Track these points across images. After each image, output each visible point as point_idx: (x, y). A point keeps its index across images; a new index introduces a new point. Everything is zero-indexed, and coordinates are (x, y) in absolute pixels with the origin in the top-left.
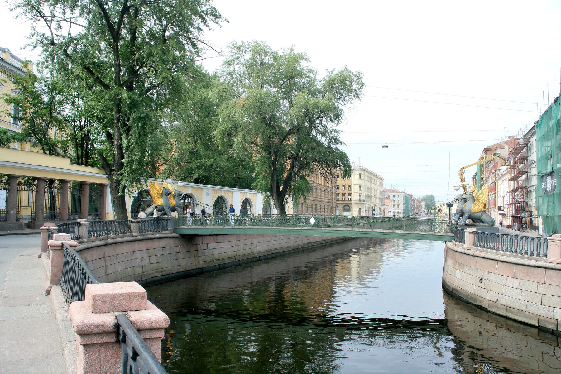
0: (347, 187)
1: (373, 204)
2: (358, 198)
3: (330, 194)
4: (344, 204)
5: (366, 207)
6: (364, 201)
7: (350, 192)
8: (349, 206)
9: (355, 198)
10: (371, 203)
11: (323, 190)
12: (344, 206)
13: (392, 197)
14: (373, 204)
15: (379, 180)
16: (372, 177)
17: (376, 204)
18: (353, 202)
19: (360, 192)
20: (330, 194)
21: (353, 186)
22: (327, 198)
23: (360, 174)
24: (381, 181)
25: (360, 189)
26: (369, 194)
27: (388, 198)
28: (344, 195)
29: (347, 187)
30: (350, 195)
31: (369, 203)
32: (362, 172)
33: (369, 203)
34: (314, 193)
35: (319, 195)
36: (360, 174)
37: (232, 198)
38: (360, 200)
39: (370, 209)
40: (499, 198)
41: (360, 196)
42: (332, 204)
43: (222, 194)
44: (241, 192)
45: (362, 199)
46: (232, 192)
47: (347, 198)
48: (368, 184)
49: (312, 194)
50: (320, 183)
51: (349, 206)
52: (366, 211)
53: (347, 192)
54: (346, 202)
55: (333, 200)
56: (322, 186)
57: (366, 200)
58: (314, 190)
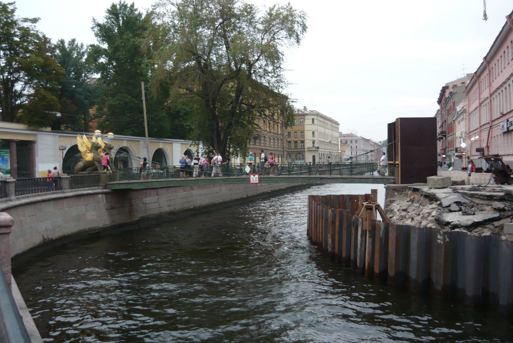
0: (299, 134)
1: (328, 151)
2: (311, 145)
3: (280, 142)
4: (297, 152)
6: (318, 148)
7: (302, 139)
8: (302, 154)
9: (308, 144)
10: (326, 150)
11: (272, 138)
12: (297, 155)
13: (349, 143)
14: (328, 151)
15: (334, 125)
16: (326, 121)
17: (331, 151)
18: (306, 149)
19: (313, 139)
20: (280, 142)
21: (305, 132)
22: (276, 147)
23: (313, 119)
24: (336, 126)
25: (313, 136)
26: (323, 140)
27: (344, 144)
28: (296, 142)
29: (299, 134)
30: (303, 142)
31: (324, 150)
32: (315, 117)
33: (324, 150)
34: (262, 142)
35: (268, 143)
36: (313, 119)
37: (172, 150)
39: (325, 156)
40: (457, 140)
41: (313, 142)
42: (282, 152)
43: (161, 146)
44: (181, 144)
46: (172, 143)
47: (299, 145)
48: (321, 129)
49: (260, 143)
50: (268, 130)
51: (302, 154)
52: (320, 158)
53: (299, 139)
54: (299, 150)
55: (283, 148)
56: (271, 134)
57: (320, 147)
58: (262, 138)
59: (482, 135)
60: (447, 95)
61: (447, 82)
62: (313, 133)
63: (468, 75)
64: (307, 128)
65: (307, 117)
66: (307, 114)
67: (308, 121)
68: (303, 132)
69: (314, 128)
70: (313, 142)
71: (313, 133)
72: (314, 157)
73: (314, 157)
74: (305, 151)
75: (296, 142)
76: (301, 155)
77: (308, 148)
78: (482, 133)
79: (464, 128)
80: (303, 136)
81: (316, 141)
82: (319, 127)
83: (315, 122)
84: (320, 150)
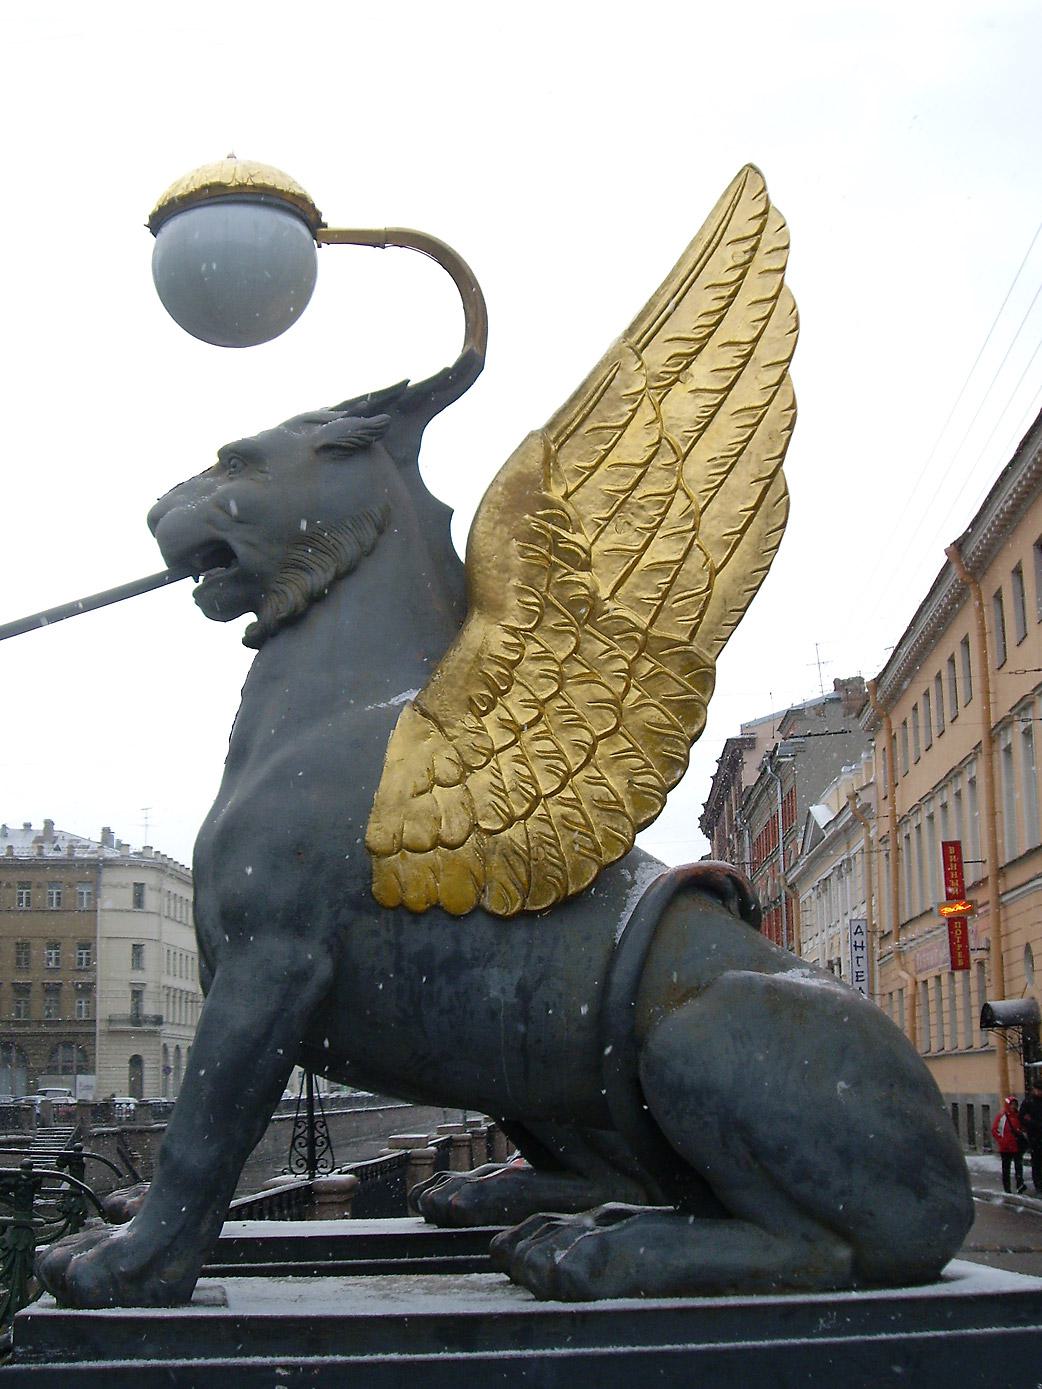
2: (125, 1008)
5: (171, 1050)
6: (158, 1020)
9: (111, 1003)
12: (54, 1051)
18: (100, 1027)
19: (138, 977)
21: (101, 946)
23: (139, 887)
30: (88, 990)
32: (149, 878)
36: (139, 887)
38: (137, 1019)
41: (137, 994)
45: (149, 1009)
53: (69, 979)
59: (1014, 924)
60: (749, 776)
61: (748, 718)
62: (137, 949)
63: (839, 684)
64: (107, 925)
65: (108, 876)
66: (109, 864)
67: (114, 896)
68: (87, 945)
69: (141, 926)
70: (137, 994)
71: (137, 949)
72: (136, 1062)
73: (136, 1062)
74: (95, 1034)
75: (53, 990)
76: (76, 1055)
77: (110, 1021)
78: (1012, 910)
79: (864, 908)
80: (87, 965)
81: (151, 987)
82: (168, 926)
83: (151, 900)
84: (167, 1029)
